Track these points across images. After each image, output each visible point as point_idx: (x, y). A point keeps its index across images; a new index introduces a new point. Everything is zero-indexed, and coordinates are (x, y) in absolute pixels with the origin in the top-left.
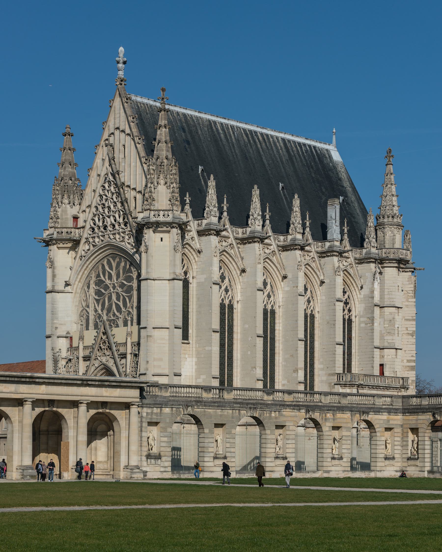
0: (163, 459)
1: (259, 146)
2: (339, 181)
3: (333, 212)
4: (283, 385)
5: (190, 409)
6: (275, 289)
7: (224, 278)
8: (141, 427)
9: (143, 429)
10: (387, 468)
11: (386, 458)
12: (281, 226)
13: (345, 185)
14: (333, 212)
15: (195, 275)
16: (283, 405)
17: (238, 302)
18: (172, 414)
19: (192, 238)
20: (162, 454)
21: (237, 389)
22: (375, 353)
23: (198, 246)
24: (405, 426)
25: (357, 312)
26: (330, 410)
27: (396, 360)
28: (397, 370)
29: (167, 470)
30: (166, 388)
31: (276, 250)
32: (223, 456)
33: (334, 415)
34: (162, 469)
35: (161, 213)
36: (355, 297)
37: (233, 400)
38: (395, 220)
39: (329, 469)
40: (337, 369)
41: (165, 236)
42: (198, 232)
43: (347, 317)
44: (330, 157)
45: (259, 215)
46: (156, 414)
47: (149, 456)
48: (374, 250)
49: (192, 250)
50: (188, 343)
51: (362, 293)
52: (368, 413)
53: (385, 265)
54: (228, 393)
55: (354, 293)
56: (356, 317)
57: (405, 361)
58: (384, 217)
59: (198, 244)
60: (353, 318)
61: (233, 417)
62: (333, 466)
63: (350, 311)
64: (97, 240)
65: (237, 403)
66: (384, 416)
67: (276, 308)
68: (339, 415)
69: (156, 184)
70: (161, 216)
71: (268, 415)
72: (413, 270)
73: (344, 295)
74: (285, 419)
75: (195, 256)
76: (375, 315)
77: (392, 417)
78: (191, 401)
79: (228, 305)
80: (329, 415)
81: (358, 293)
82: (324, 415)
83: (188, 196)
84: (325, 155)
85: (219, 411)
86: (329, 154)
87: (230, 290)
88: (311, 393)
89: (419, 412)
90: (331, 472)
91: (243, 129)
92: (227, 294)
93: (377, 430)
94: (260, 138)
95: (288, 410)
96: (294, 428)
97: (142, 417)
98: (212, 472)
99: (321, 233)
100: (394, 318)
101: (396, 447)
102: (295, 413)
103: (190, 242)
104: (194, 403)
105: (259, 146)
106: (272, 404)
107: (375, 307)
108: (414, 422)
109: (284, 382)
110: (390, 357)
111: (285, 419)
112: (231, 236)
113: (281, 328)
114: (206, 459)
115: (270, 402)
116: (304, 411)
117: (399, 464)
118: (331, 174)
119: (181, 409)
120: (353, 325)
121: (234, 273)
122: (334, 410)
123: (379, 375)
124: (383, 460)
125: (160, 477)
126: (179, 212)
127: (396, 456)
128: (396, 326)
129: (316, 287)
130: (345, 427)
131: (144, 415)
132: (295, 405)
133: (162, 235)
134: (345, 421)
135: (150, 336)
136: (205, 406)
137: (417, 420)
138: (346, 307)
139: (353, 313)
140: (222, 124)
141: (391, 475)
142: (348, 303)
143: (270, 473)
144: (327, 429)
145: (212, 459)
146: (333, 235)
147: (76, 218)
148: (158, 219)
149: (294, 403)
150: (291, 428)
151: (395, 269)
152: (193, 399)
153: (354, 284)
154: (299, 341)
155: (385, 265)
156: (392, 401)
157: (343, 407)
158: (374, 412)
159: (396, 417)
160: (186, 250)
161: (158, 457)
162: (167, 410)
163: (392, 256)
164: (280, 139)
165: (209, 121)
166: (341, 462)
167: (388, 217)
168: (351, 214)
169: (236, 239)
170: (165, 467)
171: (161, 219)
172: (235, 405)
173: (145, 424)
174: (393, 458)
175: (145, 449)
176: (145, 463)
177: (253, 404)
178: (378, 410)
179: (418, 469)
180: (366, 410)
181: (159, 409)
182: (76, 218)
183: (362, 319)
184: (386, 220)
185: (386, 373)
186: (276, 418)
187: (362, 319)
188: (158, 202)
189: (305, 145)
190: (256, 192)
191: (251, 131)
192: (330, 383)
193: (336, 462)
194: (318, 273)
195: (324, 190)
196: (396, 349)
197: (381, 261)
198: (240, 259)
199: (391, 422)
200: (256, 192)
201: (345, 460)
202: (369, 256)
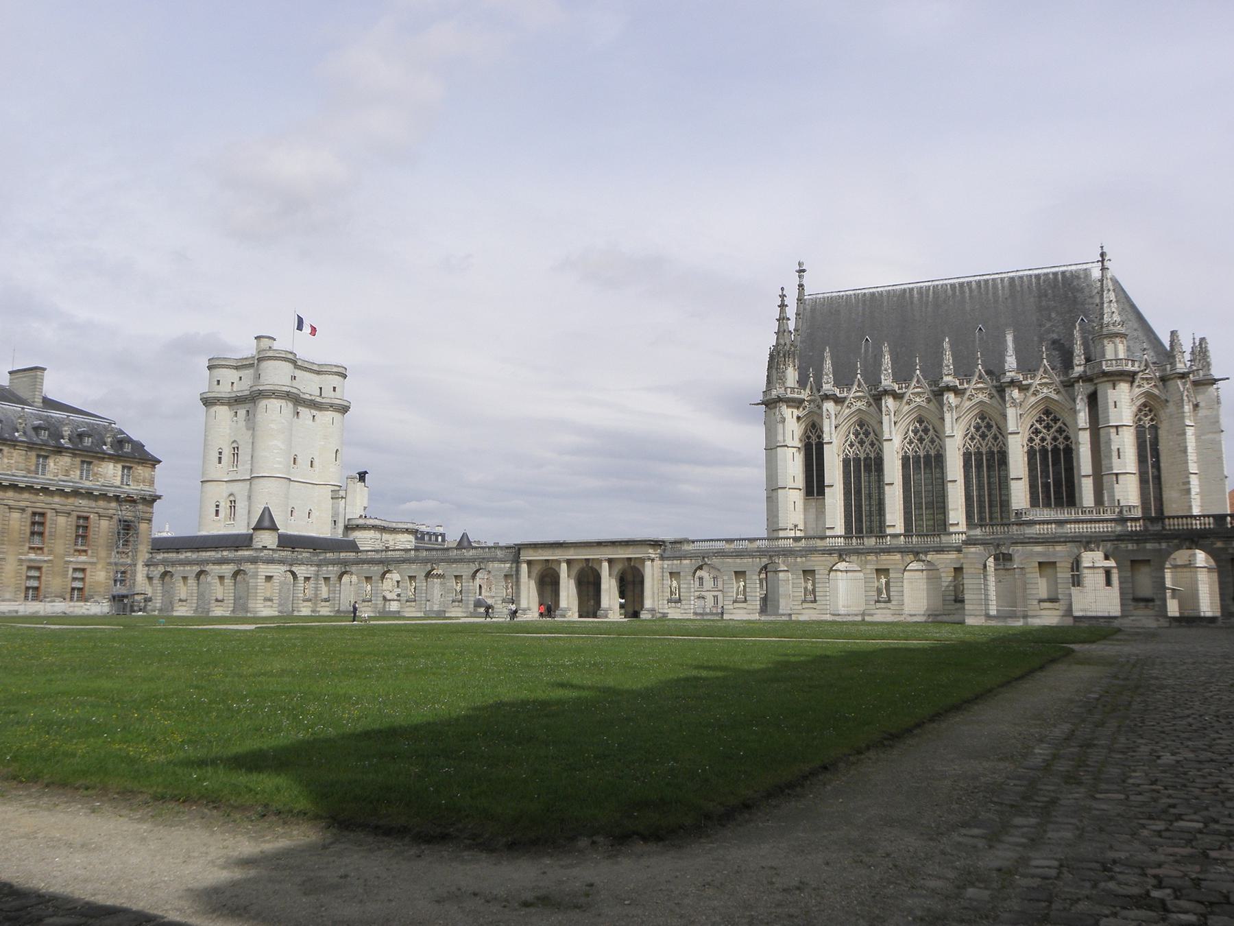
1: (967, 295)
2: (1089, 300)
43: (1061, 447)
47: (670, 601)
52: (926, 553)
63: (1067, 438)
68: (884, 557)
80: (872, 557)
84: (1078, 277)
85: (738, 561)
105: (967, 295)
107: (1081, 433)
118: (1078, 295)
128: (1114, 447)
161: (679, 601)
162: (687, 562)
163: (1096, 371)
166: (889, 605)
189: (1046, 274)
191: (961, 285)
193: (882, 605)
195: (1053, 315)
196: (1117, 474)
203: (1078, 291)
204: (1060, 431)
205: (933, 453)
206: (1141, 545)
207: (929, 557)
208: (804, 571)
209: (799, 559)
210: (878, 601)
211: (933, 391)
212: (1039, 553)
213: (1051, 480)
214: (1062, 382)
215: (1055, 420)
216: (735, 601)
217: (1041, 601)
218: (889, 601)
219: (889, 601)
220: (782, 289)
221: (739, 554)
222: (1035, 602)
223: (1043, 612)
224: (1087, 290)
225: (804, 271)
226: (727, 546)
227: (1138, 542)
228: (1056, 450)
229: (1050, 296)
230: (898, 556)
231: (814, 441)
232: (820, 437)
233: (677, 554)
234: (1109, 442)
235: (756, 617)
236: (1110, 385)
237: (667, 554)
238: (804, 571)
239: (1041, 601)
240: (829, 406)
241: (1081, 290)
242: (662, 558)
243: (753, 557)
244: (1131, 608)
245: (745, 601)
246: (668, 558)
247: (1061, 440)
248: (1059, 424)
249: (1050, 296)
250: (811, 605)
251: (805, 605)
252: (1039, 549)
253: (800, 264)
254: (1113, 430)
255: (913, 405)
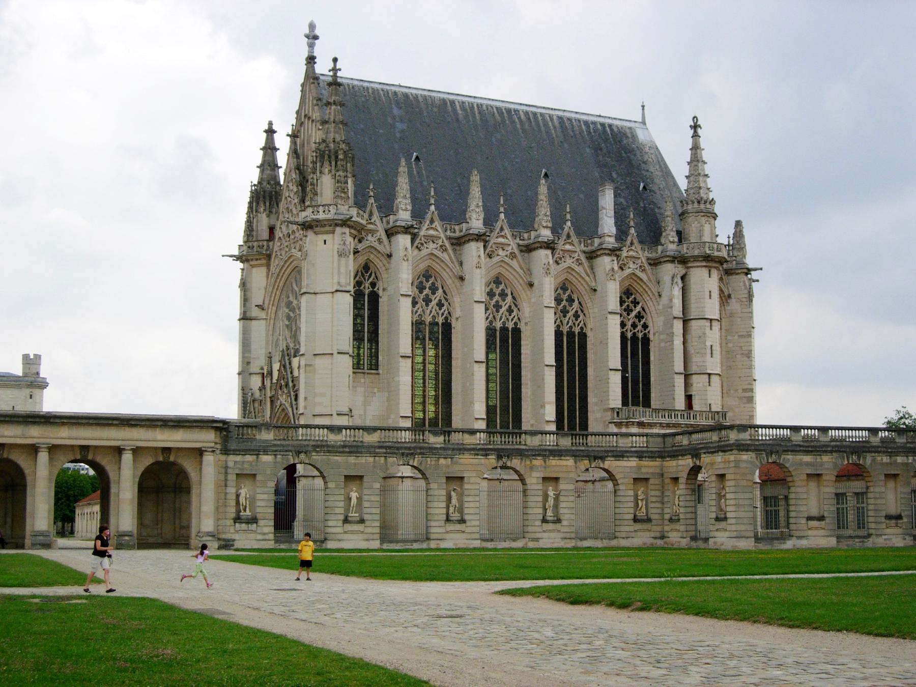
0: (261, 523)
1: (518, 126)
3: (607, 200)
4: (532, 425)
5: (302, 456)
6: (519, 302)
7: (437, 289)
8: (226, 480)
9: (229, 483)
10: (639, 534)
11: (636, 520)
12: (522, 221)
13: (652, 169)
14: (607, 200)
15: (385, 286)
16: (462, 449)
17: (457, 319)
18: (275, 462)
19: (379, 239)
20: (259, 516)
21: (457, 431)
22: (676, 380)
23: (388, 249)
24: (665, 475)
25: (656, 328)
26: (539, 455)
27: (709, 388)
28: (712, 402)
29: (267, 537)
30: (268, 429)
31: (516, 251)
32: (358, 519)
33: (545, 462)
34: (469, 536)
35: (321, 209)
36: (652, 308)
37: (376, 444)
38: (702, 206)
39: (538, 535)
40: (611, 402)
41: (328, 237)
42: (386, 231)
43: (640, 335)
44: (634, 137)
45: (478, 206)
46: (250, 463)
47: (237, 519)
48: (673, 247)
49: (379, 255)
50: (378, 374)
51: (661, 303)
52: (602, 459)
53: (690, 265)
54: (369, 434)
55: (650, 304)
56: (654, 334)
57: (740, 391)
58: (687, 204)
59: (388, 247)
60: (651, 337)
61: (374, 467)
62: (544, 531)
63: (645, 326)
64: (283, 253)
65: (380, 447)
66: (633, 462)
67: (521, 326)
68: (553, 462)
69: (318, 174)
70: (321, 212)
71: (433, 463)
72: (745, 271)
73: (621, 305)
74: (462, 467)
75: (385, 262)
76: (675, 331)
77: (646, 463)
78: (308, 445)
79: (443, 324)
80: (538, 462)
81: (656, 303)
82: (528, 463)
83: (371, 187)
84: (625, 135)
85: (352, 459)
86: (631, 133)
87: (446, 304)
88: (583, 435)
89: (678, 456)
90: (541, 541)
91: (497, 108)
92: (440, 309)
93: (619, 482)
94: (523, 117)
95: (467, 456)
96: (478, 480)
97: (226, 467)
98: (340, 540)
99: (587, 227)
100: (704, 334)
101: (652, 505)
102: (481, 460)
103: (376, 245)
104: (310, 449)
105: (518, 126)
106: (441, 448)
107: (675, 321)
108: (674, 469)
109: (532, 422)
110: (701, 385)
111: (462, 467)
112: (442, 236)
113: (528, 352)
114: (330, 523)
115: (439, 446)
116: (493, 457)
117: (659, 528)
118: (632, 157)
119: (290, 457)
120: (652, 344)
121: (449, 282)
122: (544, 456)
123: (386, 394)
124: (632, 522)
125: (256, 547)
126: (347, 207)
127: (653, 517)
128: (708, 344)
129: (586, 297)
130: (565, 478)
131: (231, 464)
132: (480, 449)
133: (325, 237)
134: (564, 469)
135: (310, 365)
136: (329, 452)
137: (678, 466)
138: (640, 321)
139: (651, 328)
140: (463, 103)
141: (645, 544)
142: (643, 317)
143: (438, 542)
144: (534, 481)
145: (340, 523)
146: (603, 229)
147: (272, 229)
148: (318, 217)
149: (479, 447)
150: (472, 480)
151: (704, 269)
152: (311, 443)
153: (649, 292)
154: (401, 359)
155: (690, 265)
156: (647, 442)
157: (560, 451)
158: (613, 456)
159: (652, 463)
160: (372, 256)
161: (254, 520)
162: (267, 458)
163: (696, 252)
164: (555, 118)
165: (444, 100)
166: (558, 526)
167: (693, 203)
168: (655, 204)
169: (450, 238)
170: (264, 534)
171: (321, 216)
172: (377, 450)
173: (232, 478)
174: (649, 520)
175: (232, 511)
176: (232, 530)
177: (409, 448)
178: (620, 455)
179: (680, 534)
180: (601, 455)
181: (255, 457)
182: (272, 229)
183: (662, 337)
184: (690, 207)
185: (696, 406)
186: (448, 466)
187: (662, 337)
188: (322, 196)
189: (594, 123)
190: (475, 177)
191: (509, 111)
192: (605, 422)
193: (551, 526)
194: (587, 278)
195: (614, 175)
196: (709, 374)
197: (683, 260)
198: (456, 264)
199: (644, 470)
200: (475, 177)
201: (565, 523)
202: (604, 246)
203: (630, 152)
204: (639, 317)
205: (510, 325)
206: (894, 458)
207: (607, 464)
208: (448, 478)
209: (442, 461)
210: (544, 520)
211: (519, 245)
212: (808, 464)
213: (629, 375)
214: (648, 259)
215: (636, 303)
216: (346, 520)
217: (810, 518)
218: (558, 521)
219: (558, 521)
220: (335, 60)
221: (354, 449)
222: (804, 521)
223: (810, 533)
224: (638, 153)
225: (316, 38)
226: (332, 438)
227: (891, 454)
228: (634, 337)
229: (605, 151)
230: (570, 462)
231: (367, 289)
232: (373, 285)
233: (249, 445)
234: (702, 337)
235: (376, 544)
236: (705, 271)
237: (233, 445)
238: (448, 478)
239: (810, 518)
240: (403, 241)
241: (632, 151)
242: (226, 451)
243: (376, 455)
244: (884, 526)
245: (362, 521)
246: (236, 452)
247: (639, 327)
248: (638, 308)
249: (605, 151)
250: (458, 527)
251: (451, 527)
252: (807, 458)
253: (312, 26)
254: (708, 324)
255: (496, 259)
